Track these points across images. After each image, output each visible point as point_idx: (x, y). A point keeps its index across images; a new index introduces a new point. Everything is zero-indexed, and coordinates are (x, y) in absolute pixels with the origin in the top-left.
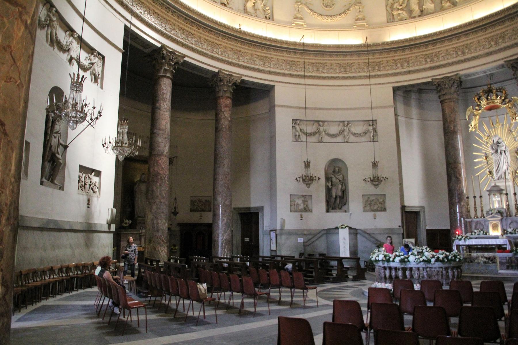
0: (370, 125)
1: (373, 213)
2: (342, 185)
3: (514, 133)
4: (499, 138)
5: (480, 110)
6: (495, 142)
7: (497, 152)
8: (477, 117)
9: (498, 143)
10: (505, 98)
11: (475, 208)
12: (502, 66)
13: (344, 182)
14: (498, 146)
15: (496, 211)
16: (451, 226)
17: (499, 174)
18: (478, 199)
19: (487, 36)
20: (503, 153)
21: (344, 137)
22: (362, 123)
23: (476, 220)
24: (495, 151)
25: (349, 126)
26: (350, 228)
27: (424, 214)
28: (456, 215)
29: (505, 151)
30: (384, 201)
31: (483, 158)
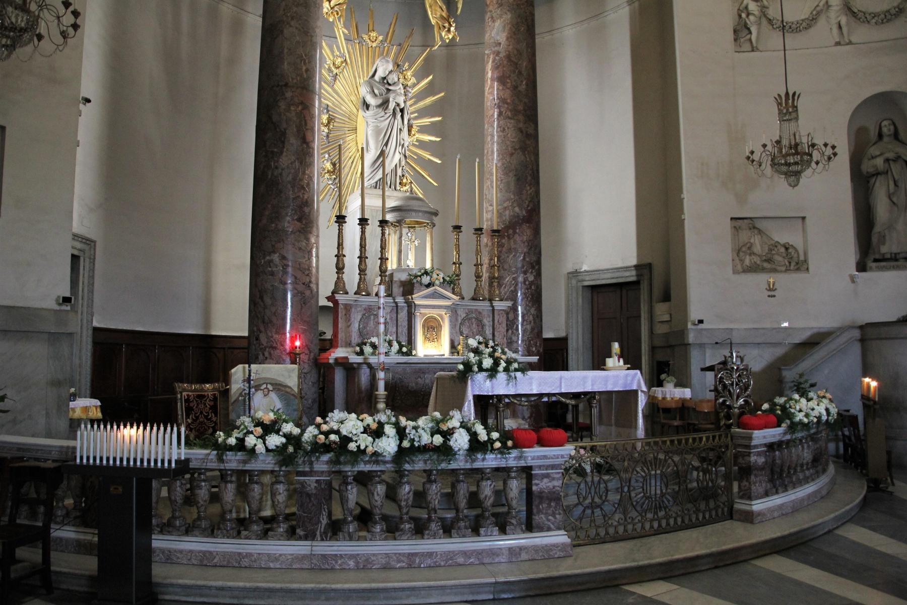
3: (409, 74)
6: (377, 78)
7: (384, 104)
14: (389, 90)
23: (364, 300)
24: (380, 101)
27: (92, 270)
29: (402, 111)
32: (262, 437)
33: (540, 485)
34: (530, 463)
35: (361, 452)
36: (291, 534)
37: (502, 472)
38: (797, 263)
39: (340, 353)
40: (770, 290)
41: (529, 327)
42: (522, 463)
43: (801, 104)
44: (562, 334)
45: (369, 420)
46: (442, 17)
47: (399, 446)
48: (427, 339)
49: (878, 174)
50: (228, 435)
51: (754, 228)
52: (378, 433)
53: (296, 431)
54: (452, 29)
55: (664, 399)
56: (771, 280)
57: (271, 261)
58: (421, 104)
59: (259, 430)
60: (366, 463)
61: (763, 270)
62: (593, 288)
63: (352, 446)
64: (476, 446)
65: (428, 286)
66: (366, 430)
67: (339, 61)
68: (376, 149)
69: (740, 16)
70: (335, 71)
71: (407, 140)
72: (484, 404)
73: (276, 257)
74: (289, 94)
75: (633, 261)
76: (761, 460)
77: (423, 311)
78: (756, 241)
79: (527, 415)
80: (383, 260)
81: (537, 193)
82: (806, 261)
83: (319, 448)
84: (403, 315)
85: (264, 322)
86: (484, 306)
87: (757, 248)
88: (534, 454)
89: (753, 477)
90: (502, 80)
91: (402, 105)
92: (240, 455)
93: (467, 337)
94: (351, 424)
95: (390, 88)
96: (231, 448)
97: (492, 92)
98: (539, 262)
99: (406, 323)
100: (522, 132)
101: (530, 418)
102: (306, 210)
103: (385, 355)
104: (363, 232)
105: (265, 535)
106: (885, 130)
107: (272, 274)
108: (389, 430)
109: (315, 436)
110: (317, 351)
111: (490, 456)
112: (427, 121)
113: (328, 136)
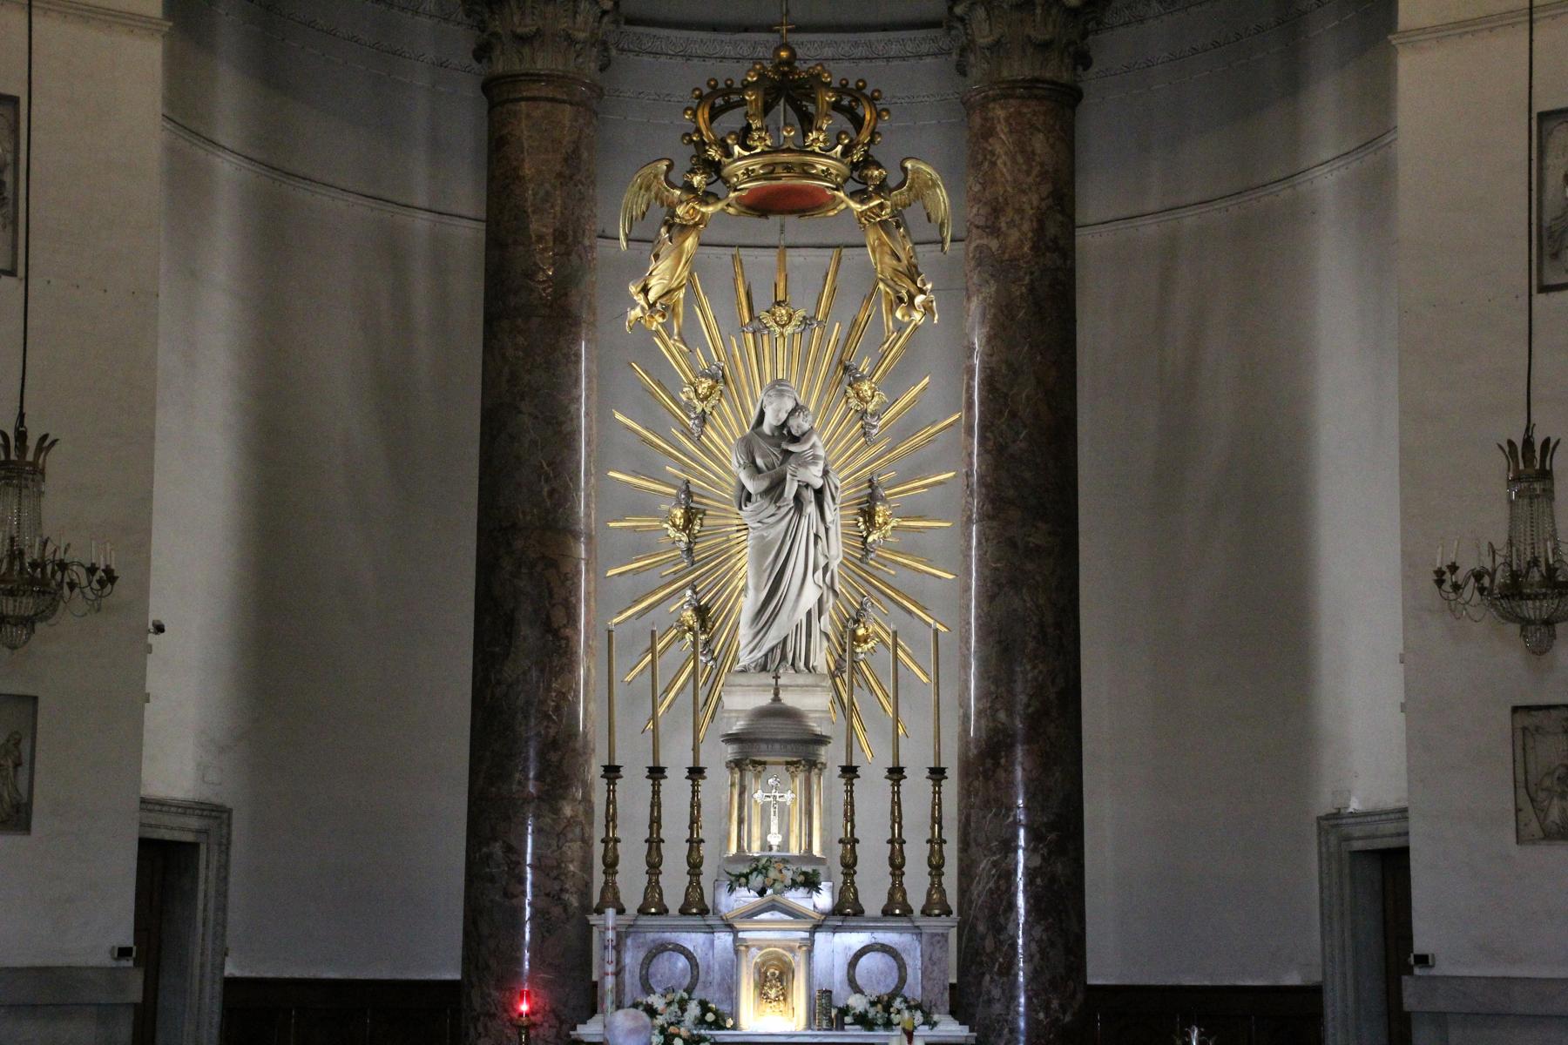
3: (865, 387)
4: (797, 409)
5: (707, 197)
6: (766, 428)
7: (774, 490)
8: (690, 243)
9: (786, 435)
10: (869, 161)
11: (655, 843)
14: (787, 454)
15: (788, 875)
16: (471, 958)
17: (772, 639)
18: (676, 788)
20: (811, 509)
24: (765, 484)
27: (225, 867)
28: (522, 881)
29: (819, 493)
31: (669, 517)
44: (1316, 978)
48: (762, 995)
57: (490, 856)
68: (757, 589)
70: (699, 406)
73: (497, 848)
74: (519, 544)
85: (477, 967)
91: (818, 483)
95: (792, 448)
100: (1012, 543)
113: (689, 551)
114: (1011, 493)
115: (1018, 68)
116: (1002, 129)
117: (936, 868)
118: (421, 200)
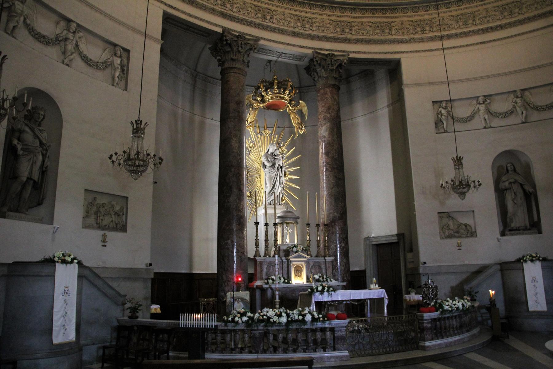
0: (115, 55)
1: (101, 233)
2: (44, 156)
6: (269, 153)
7: (273, 166)
12: (300, 57)
13: (49, 152)
14: (275, 158)
19: (294, 13)
21: (64, 53)
22: (101, 43)
23: (268, 259)
24: (271, 164)
25: (78, 35)
26: (79, 263)
29: (281, 167)
30: (123, 212)
32: (240, 318)
33: (338, 334)
34: (333, 326)
35: (275, 322)
36: (250, 352)
37: (323, 330)
38: (471, 233)
39: (258, 283)
40: (459, 246)
41: (343, 268)
42: (330, 326)
43: (464, 161)
44: (363, 268)
45: (277, 311)
46: (298, 123)
47: (287, 320)
48: (296, 275)
49: (506, 189)
50: (228, 317)
51: (450, 217)
52: (280, 315)
53: (252, 315)
54: (303, 128)
55: (410, 300)
56: (459, 242)
58: (290, 161)
59: (239, 315)
60: (276, 326)
61: (455, 237)
62: (378, 245)
63: (271, 320)
64: (314, 320)
65: (296, 252)
66: (276, 314)
67: (251, 145)
69: (438, 116)
70: (250, 149)
71: (283, 179)
72: (320, 305)
73: (229, 242)
74: (233, 170)
75: (395, 232)
76: (429, 325)
77: (294, 263)
78: (451, 223)
79: (343, 309)
80: (276, 241)
81: (345, 205)
82: (475, 232)
83: (260, 321)
84: (285, 265)
86: (321, 259)
87: (452, 227)
88: (335, 323)
89: (425, 332)
90: (327, 154)
91: (281, 165)
92: (233, 324)
93: (314, 275)
94: (271, 313)
96: (230, 322)
97: (323, 159)
98: (347, 237)
99: (286, 269)
100: (336, 177)
101: (345, 310)
102: (242, 220)
103: (278, 284)
104: (267, 229)
105: (241, 353)
106: (509, 168)
107: (228, 249)
108: (284, 314)
109: (259, 317)
110: (247, 282)
111: (319, 323)
112: (293, 169)
114: (335, 166)
115: (332, 82)
116: (329, 93)
117: (318, 246)
118: (180, 107)
